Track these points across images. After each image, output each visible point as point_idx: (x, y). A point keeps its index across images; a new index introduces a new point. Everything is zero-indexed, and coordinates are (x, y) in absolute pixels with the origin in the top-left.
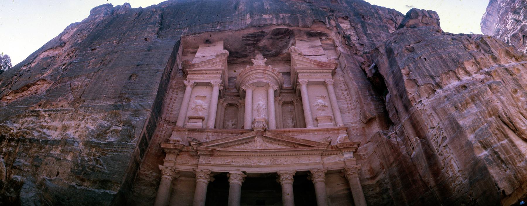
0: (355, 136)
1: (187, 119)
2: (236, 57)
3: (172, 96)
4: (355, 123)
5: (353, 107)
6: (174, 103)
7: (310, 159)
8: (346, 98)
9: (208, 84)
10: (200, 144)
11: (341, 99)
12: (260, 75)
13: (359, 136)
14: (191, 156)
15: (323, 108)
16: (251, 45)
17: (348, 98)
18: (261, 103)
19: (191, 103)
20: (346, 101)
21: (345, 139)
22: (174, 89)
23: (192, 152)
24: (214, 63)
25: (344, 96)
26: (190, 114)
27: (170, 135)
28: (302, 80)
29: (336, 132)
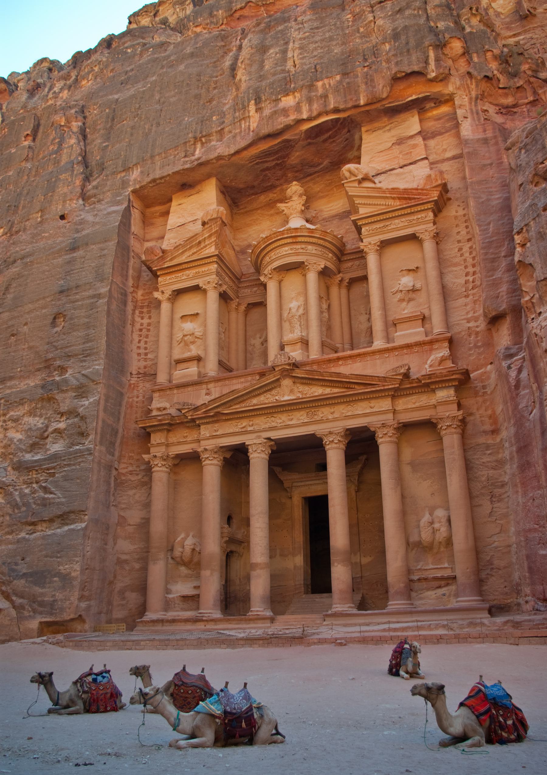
0: (470, 349)
1: (173, 363)
2: (253, 194)
3: (142, 324)
4: (476, 319)
5: (478, 283)
6: (147, 336)
7: (372, 405)
8: (465, 260)
9: (196, 288)
10: (196, 409)
11: (456, 265)
12: (286, 250)
13: (479, 347)
14: (188, 427)
15: (411, 295)
16: (274, 167)
17: (470, 261)
18: (294, 305)
19: (175, 330)
20: (466, 267)
21: (440, 363)
22: (142, 307)
23: (187, 422)
24: (200, 243)
25: (462, 255)
26: (178, 354)
27: (151, 399)
28: (370, 241)
29: (426, 347)
